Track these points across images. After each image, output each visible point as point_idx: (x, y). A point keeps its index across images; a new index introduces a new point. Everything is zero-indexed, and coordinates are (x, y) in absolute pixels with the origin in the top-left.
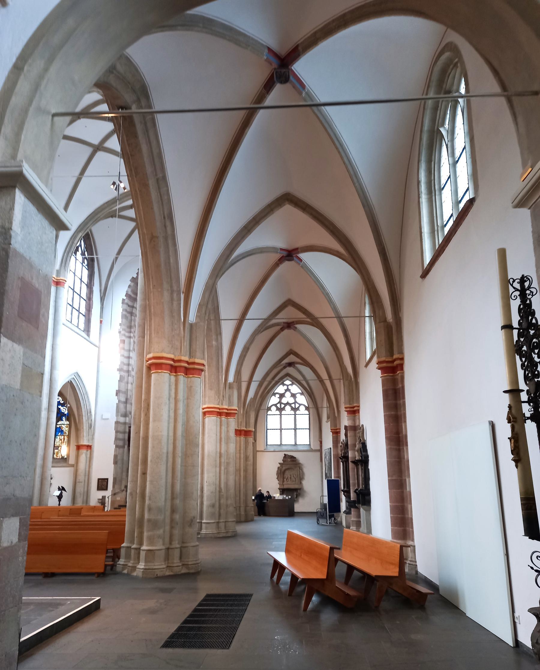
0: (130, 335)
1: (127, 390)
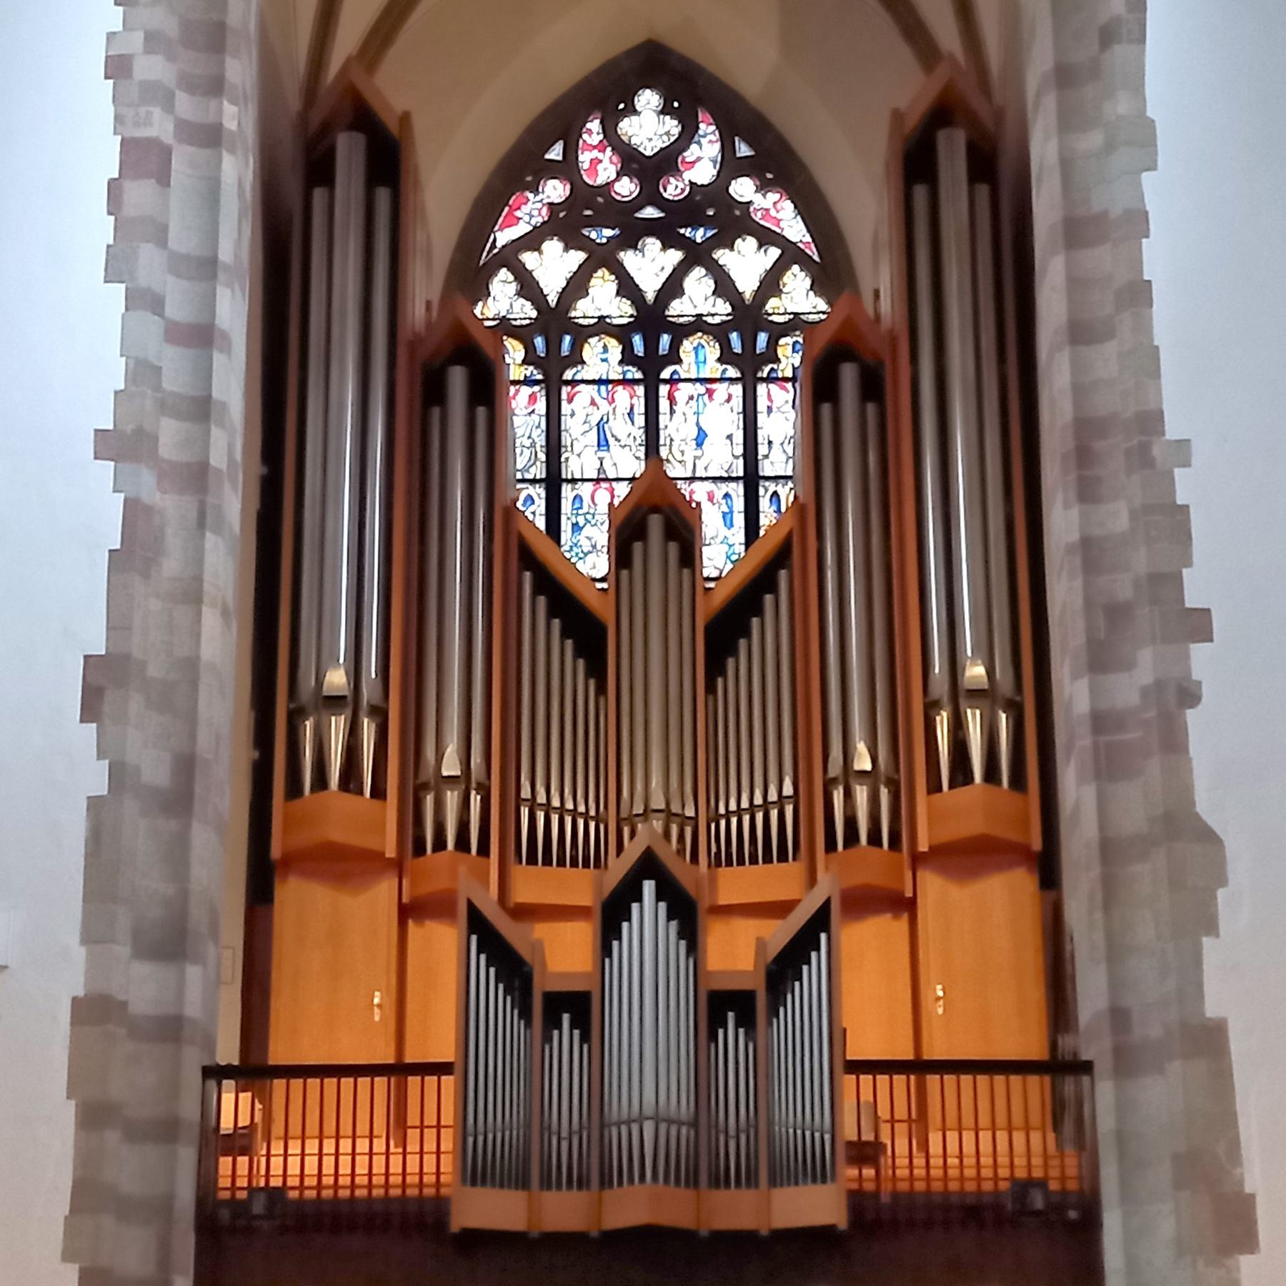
0: (211, 118)
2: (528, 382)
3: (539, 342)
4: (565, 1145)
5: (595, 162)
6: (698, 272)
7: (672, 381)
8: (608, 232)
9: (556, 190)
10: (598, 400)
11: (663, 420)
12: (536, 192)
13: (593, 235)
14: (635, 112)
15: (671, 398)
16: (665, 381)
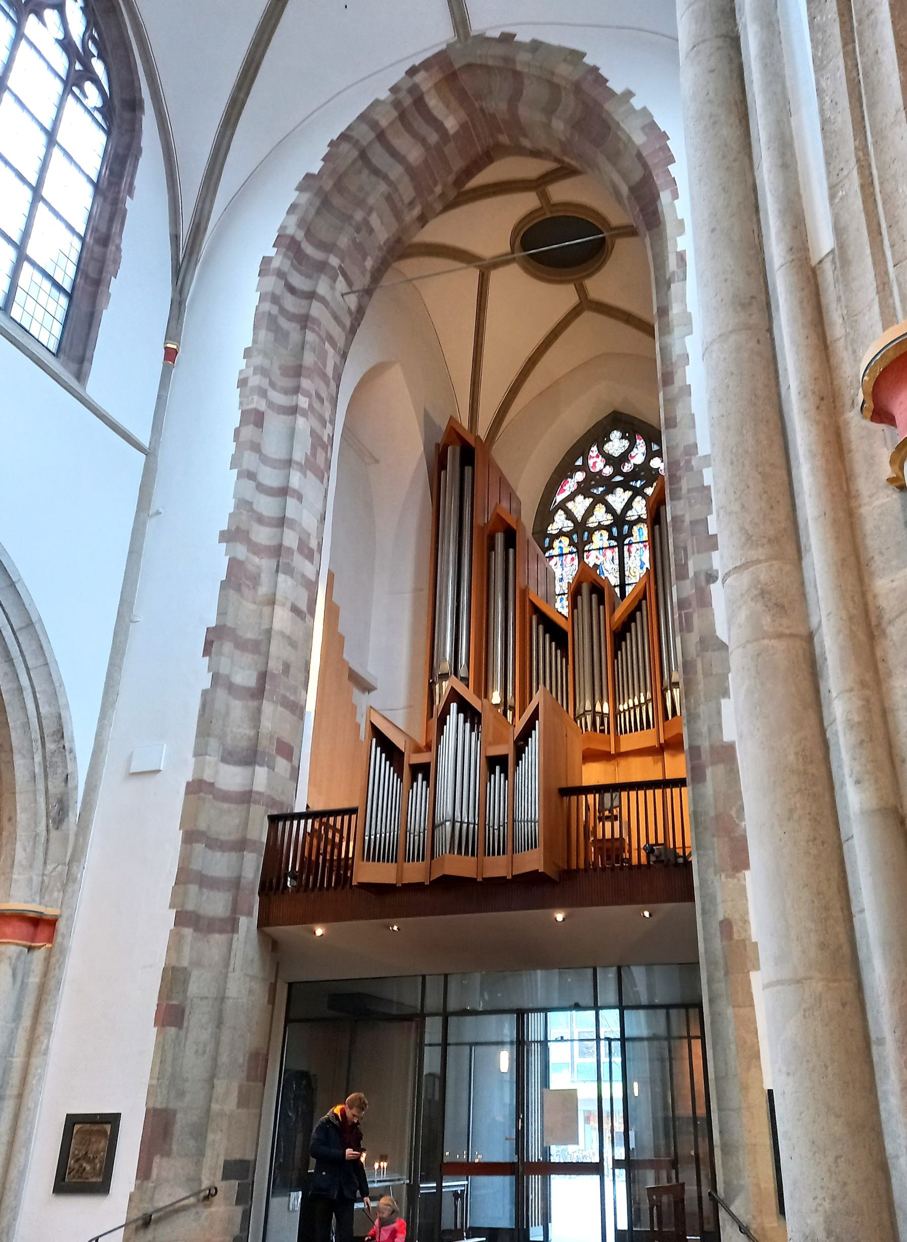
1: (269, 632)
2: (571, 553)
3: (575, 537)
4: (416, 838)
5: (595, 463)
6: (639, 498)
7: (630, 544)
8: (601, 489)
9: (580, 476)
10: (599, 556)
11: (626, 560)
12: (572, 478)
13: (595, 491)
14: (610, 440)
15: (629, 551)
16: (626, 545)
